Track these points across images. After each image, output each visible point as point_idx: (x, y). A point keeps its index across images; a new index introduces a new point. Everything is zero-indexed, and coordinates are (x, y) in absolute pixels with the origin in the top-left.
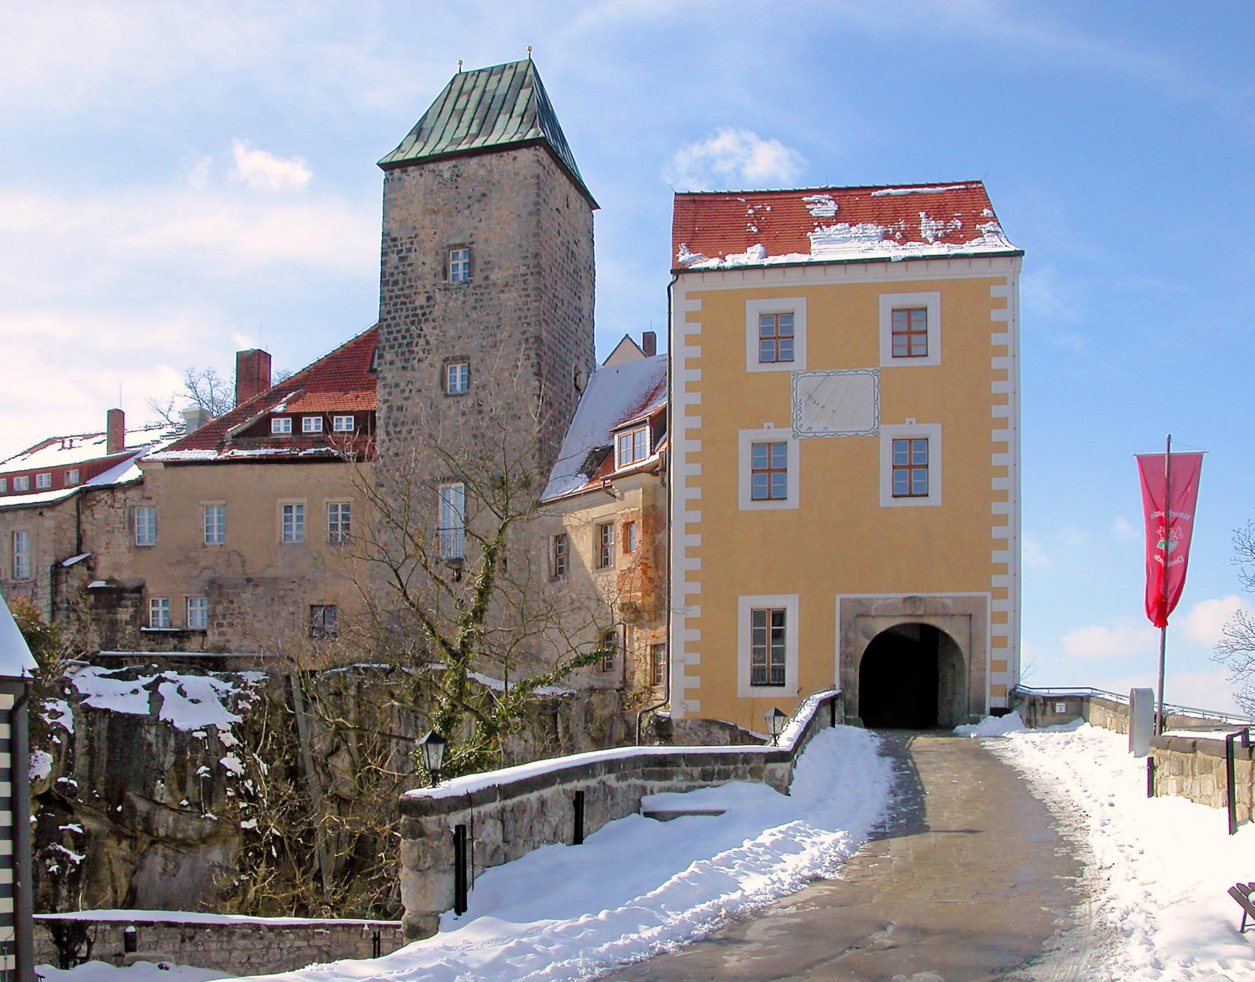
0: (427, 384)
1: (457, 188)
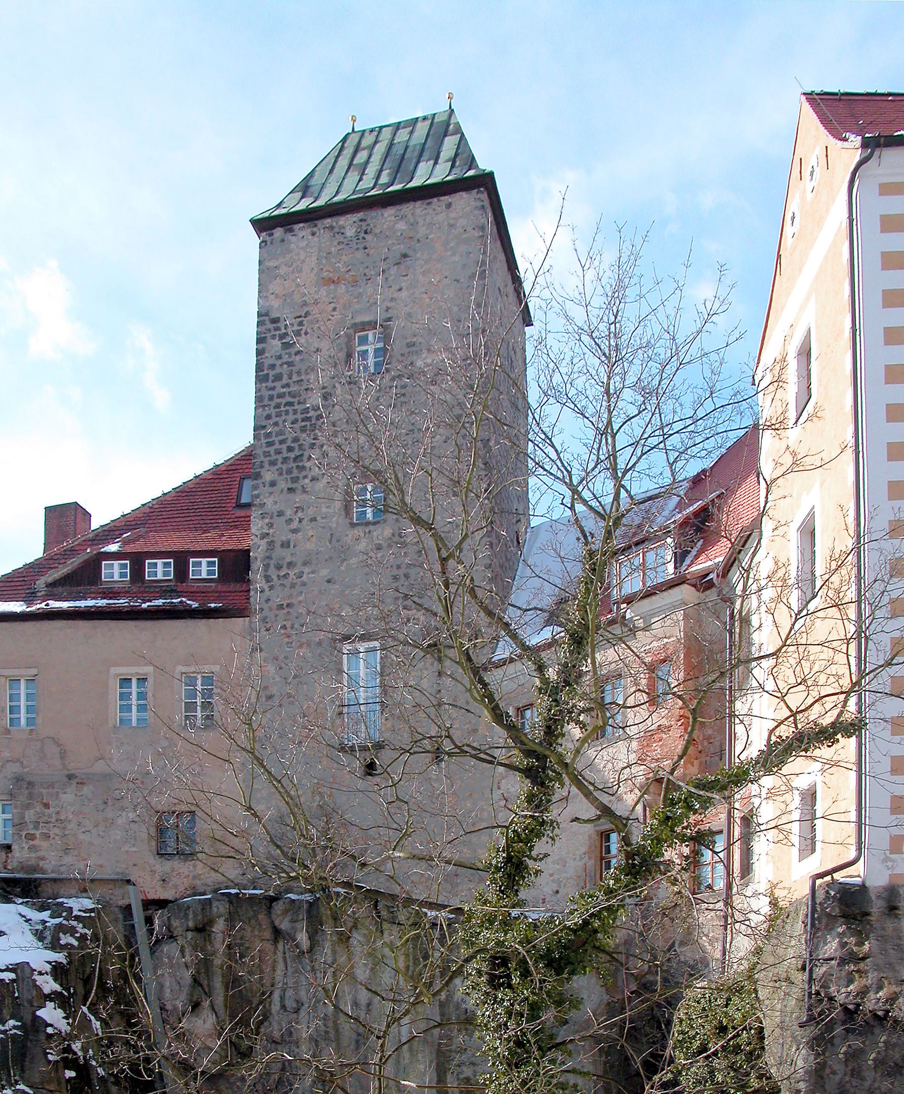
0: (324, 510)
1: (365, 248)
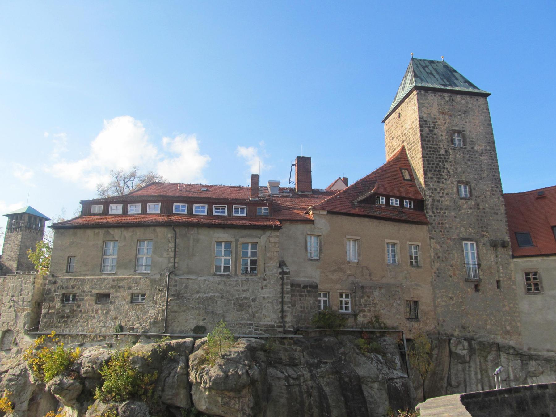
0: (450, 191)
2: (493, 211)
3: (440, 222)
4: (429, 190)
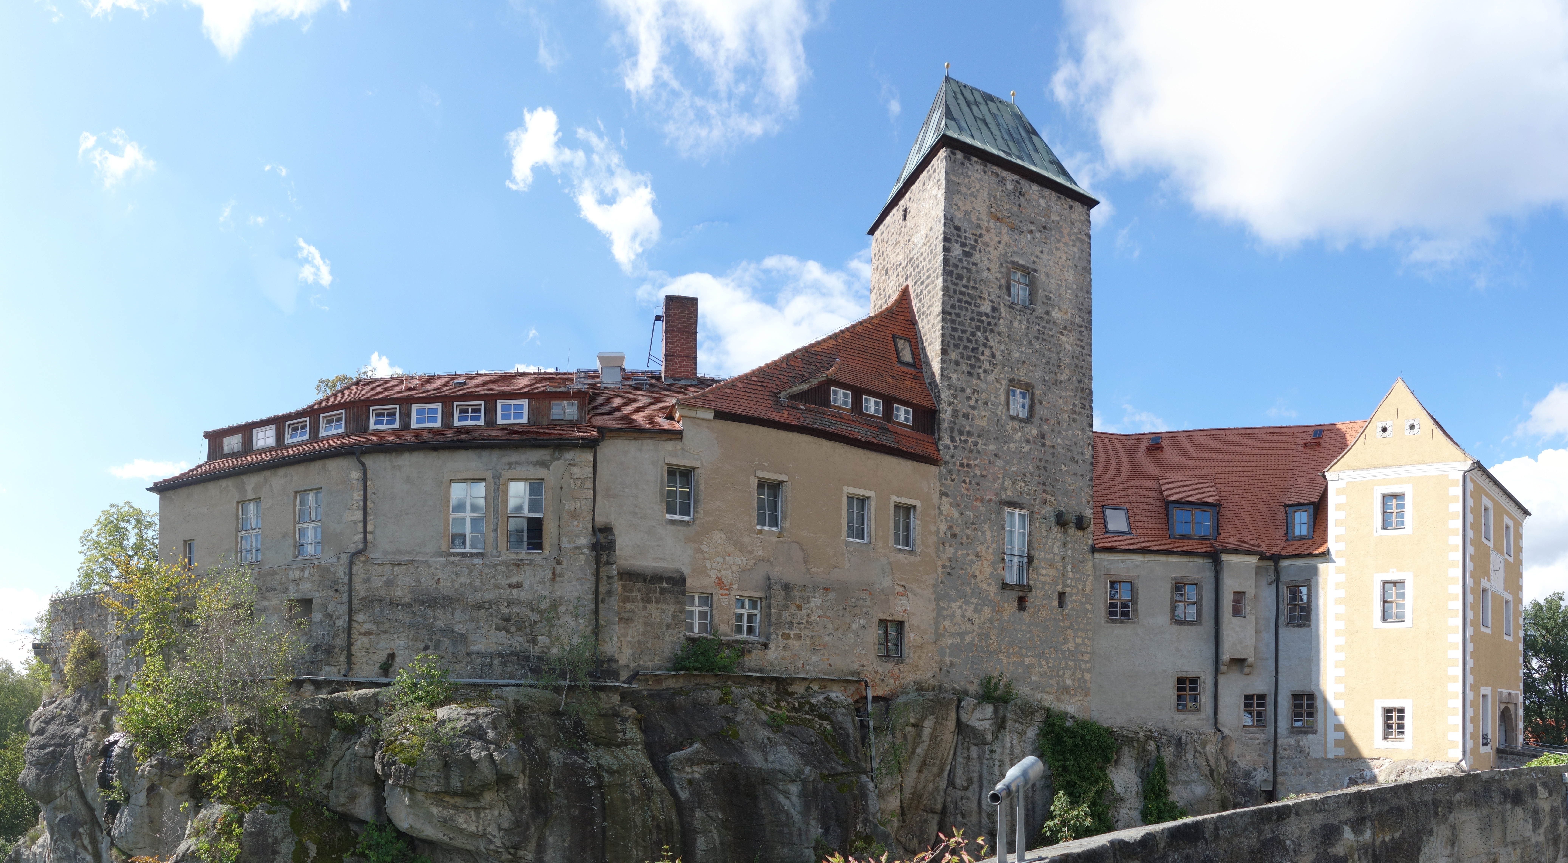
2: (1069, 455)
3: (965, 461)
4: (950, 388)
